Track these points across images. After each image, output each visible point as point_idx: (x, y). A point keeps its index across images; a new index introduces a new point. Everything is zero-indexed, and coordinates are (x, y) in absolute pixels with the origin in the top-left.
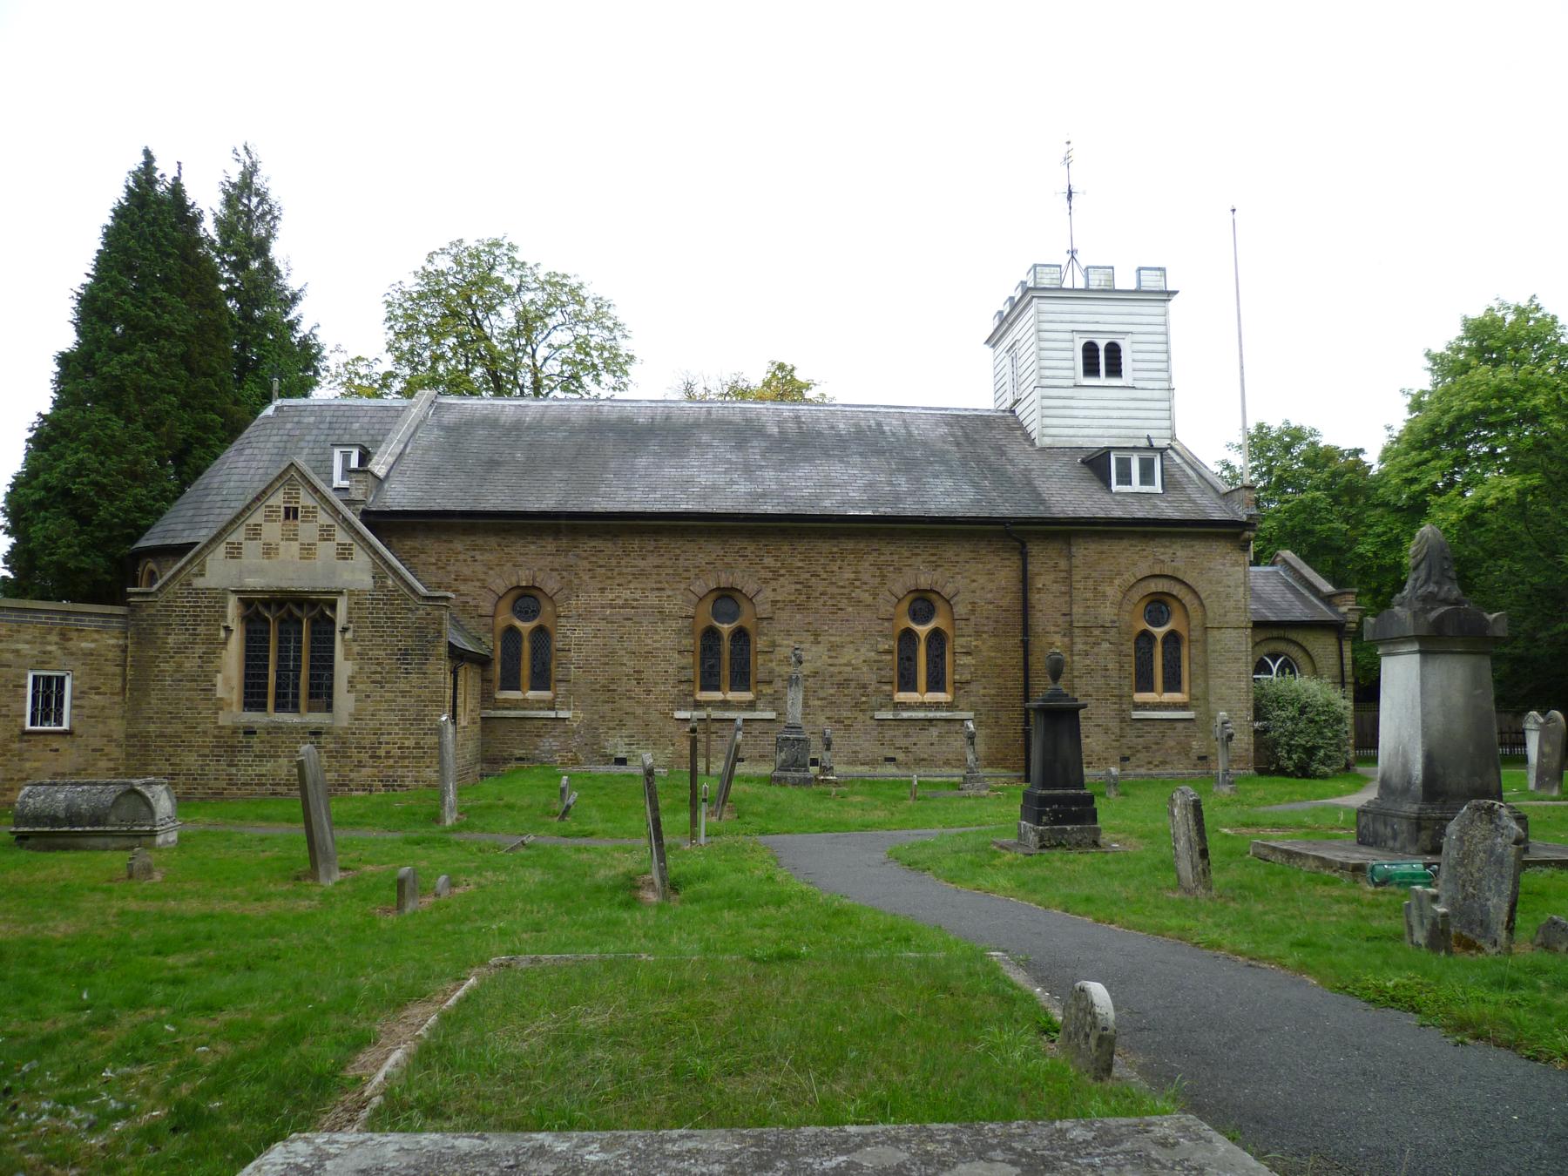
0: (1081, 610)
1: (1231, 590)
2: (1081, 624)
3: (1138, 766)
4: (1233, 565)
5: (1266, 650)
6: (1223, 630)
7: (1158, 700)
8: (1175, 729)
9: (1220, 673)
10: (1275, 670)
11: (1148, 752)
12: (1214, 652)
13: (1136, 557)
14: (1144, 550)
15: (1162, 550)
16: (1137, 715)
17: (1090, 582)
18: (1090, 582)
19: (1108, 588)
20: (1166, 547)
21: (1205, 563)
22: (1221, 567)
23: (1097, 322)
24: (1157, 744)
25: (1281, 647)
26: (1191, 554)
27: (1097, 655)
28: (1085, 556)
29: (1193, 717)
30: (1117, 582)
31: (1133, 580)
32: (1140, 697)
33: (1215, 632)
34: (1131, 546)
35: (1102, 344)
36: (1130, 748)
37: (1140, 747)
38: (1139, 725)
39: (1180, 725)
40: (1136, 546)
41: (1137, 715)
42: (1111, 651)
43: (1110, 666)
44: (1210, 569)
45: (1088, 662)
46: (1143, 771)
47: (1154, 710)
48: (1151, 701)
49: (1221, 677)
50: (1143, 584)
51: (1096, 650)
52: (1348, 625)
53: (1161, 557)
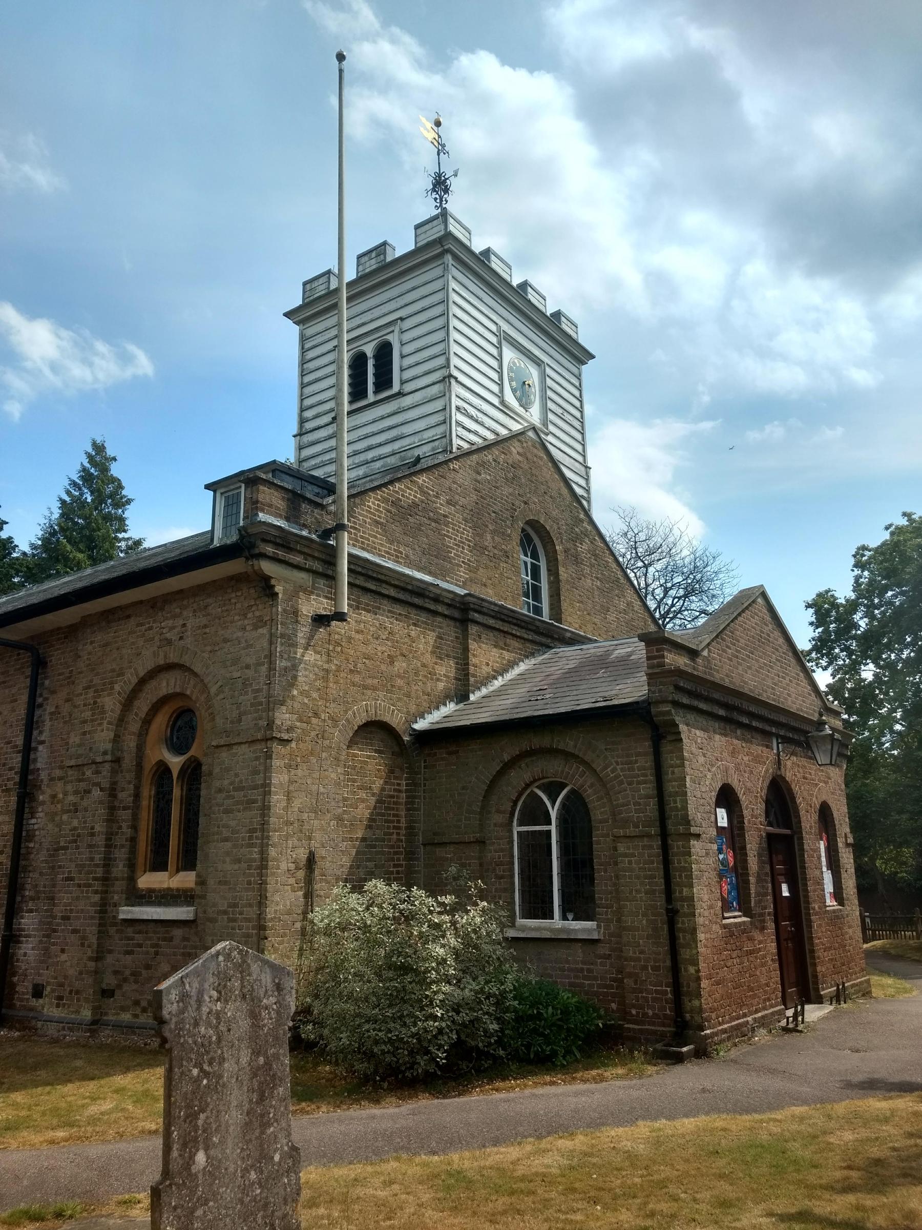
0: (77, 740)
1: (250, 673)
2: (72, 763)
3: (123, 1009)
4: (256, 627)
5: (527, 777)
6: (235, 750)
7: (165, 886)
8: (171, 939)
9: (226, 833)
10: (553, 814)
11: (136, 982)
12: (220, 791)
13: (141, 642)
14: (151, 628)
15: (170, 623)
16: (128, 912)
17: (91, 693)
18: (91, 693)
19: (107, 699)
20: (175, 617)
21: (221, 632)
22: (240, 634)
23: (363, 324)
24: (148, 967)
25: (554, 768)
26: (204, 621)
27: (86, 810)
28: (89, 654)
29: (191, 917)
30: (117, 687)
31: (134, 680)
32: (148, 881)
33: (224, 755)
34: (138, 625)
35: (369, 350)
36: (116, 973)
37: (127, 972)
38: (130, 931)
39: (178, 932)
40: (142, 625)
41: (128, 912)
42: (101, 802)
43: (98, 828)
44: (226, 641)
45: (75, 823)
46: (126, 1017)
47: (159, 904)
48: (156, 886)
49: (226, 840)
50: (153, 683)
51: (85, 803)
52: (654, 710)
53: (168, 635)
